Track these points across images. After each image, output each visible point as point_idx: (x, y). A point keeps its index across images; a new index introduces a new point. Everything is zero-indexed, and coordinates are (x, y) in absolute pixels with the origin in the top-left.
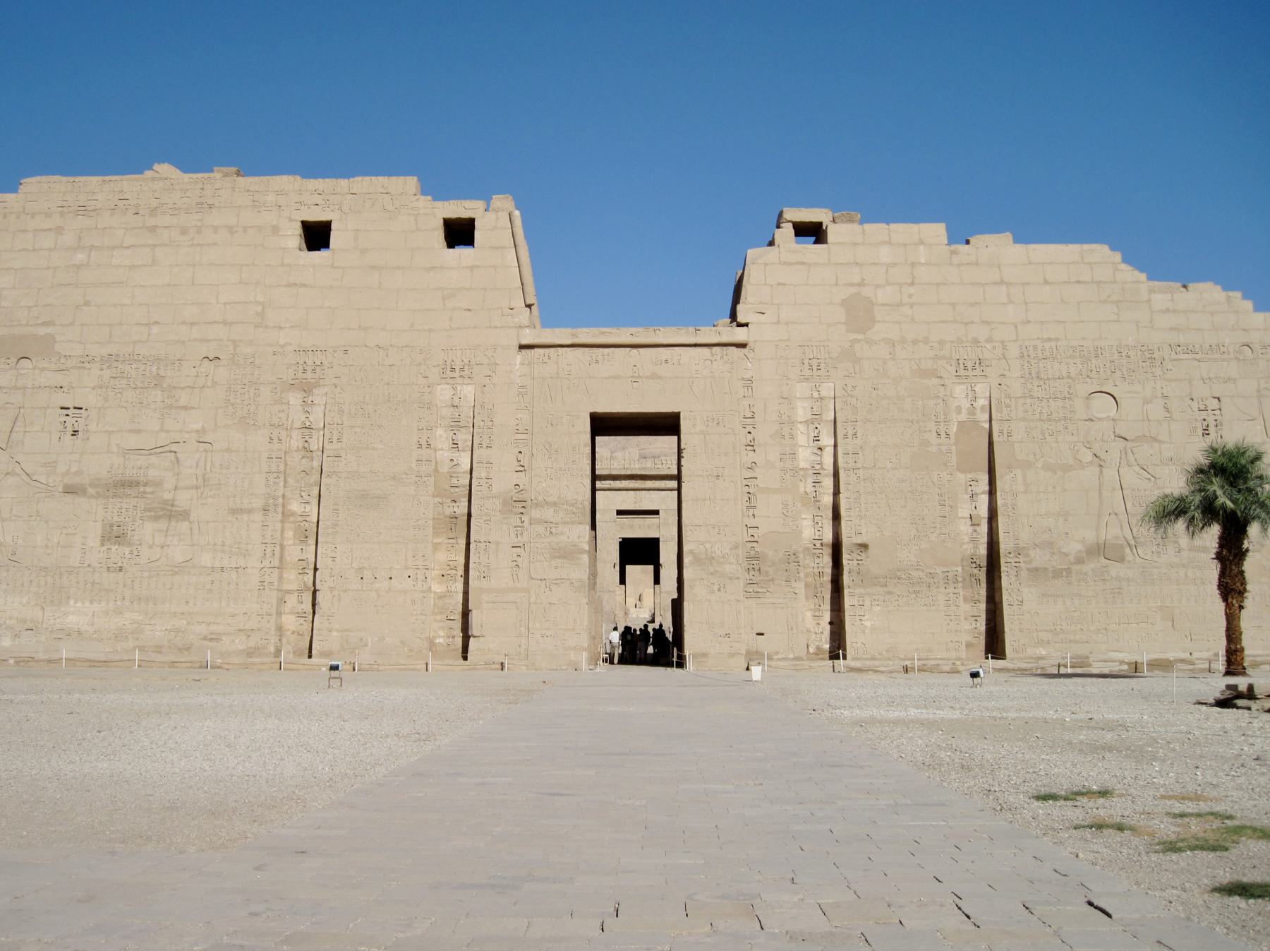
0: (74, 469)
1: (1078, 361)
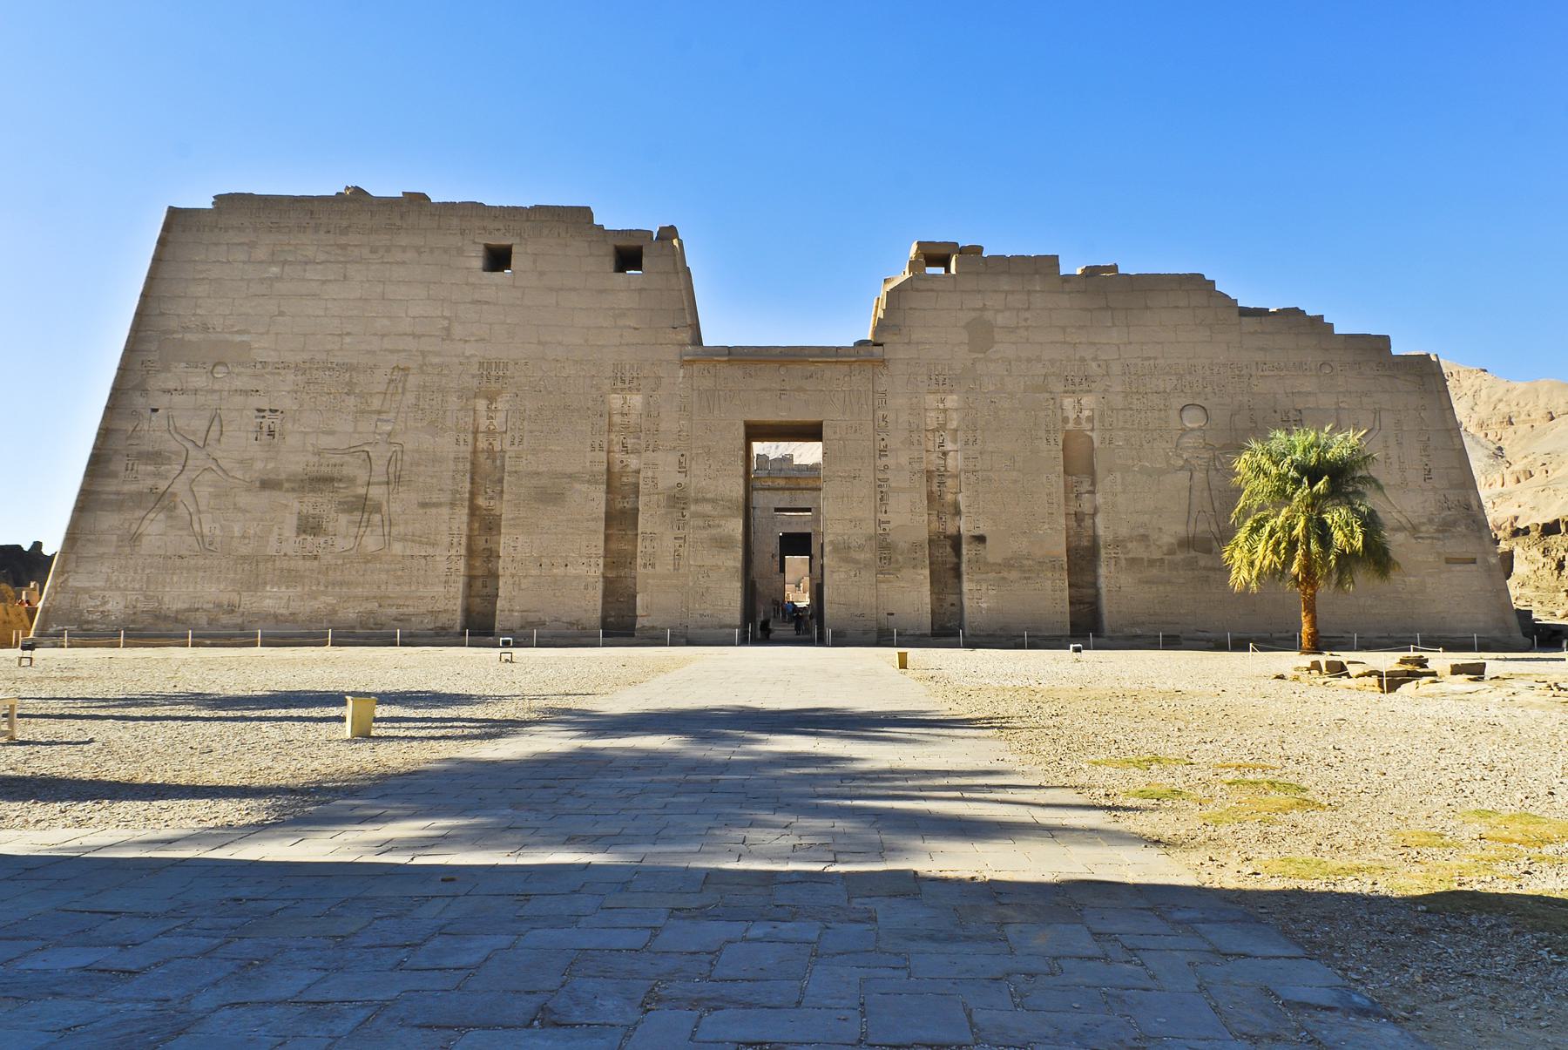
1: (1174, 378)
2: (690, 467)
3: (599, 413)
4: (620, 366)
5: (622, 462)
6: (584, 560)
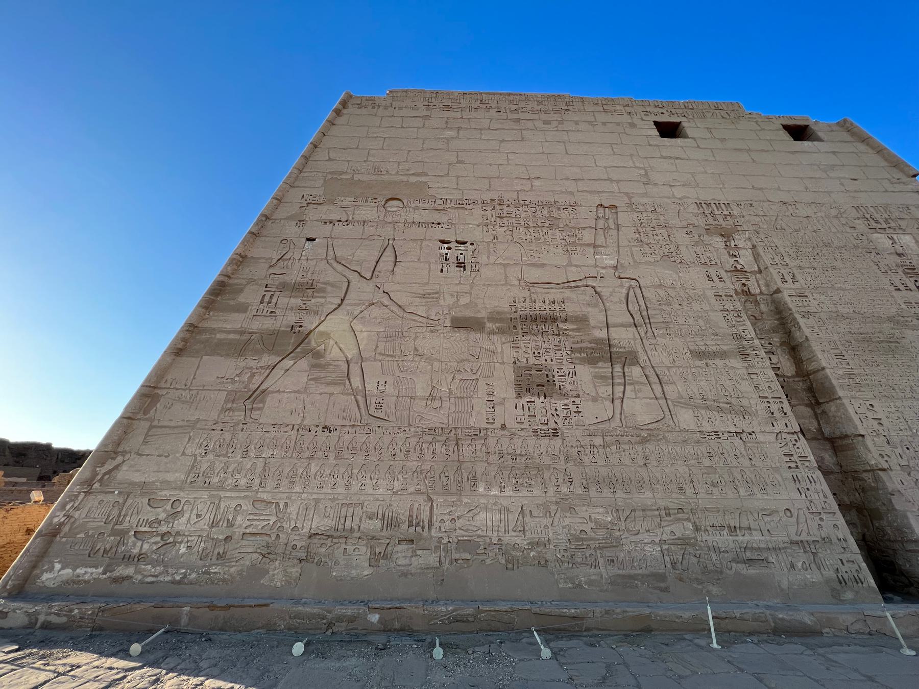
0: (464, 300)
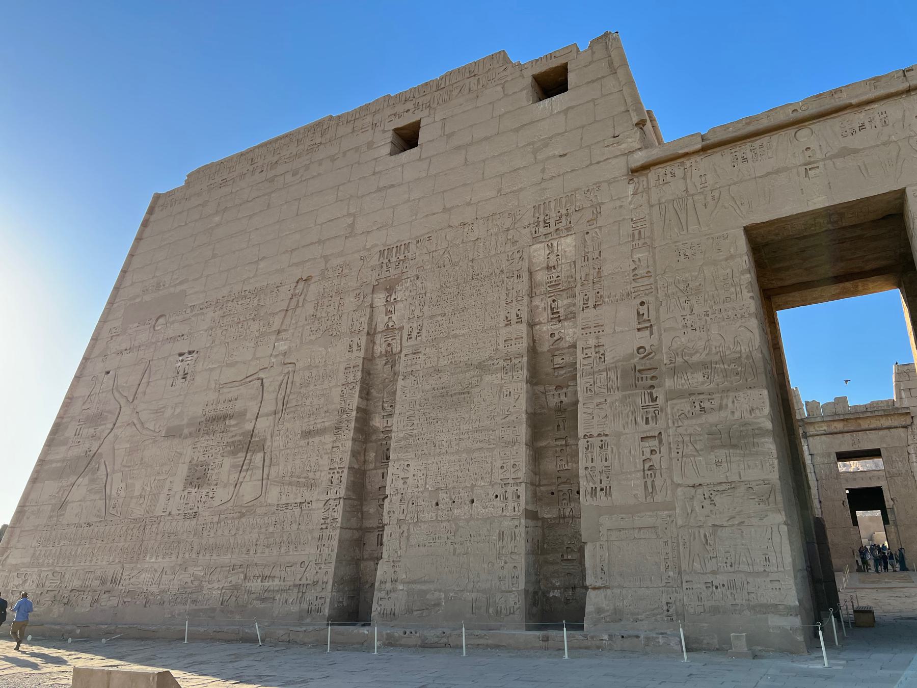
0: (178, 410)
2: (658, 318)
3: (516, 274)
4: (542, 207)
5: (552, 335)
6: (499, 491)
